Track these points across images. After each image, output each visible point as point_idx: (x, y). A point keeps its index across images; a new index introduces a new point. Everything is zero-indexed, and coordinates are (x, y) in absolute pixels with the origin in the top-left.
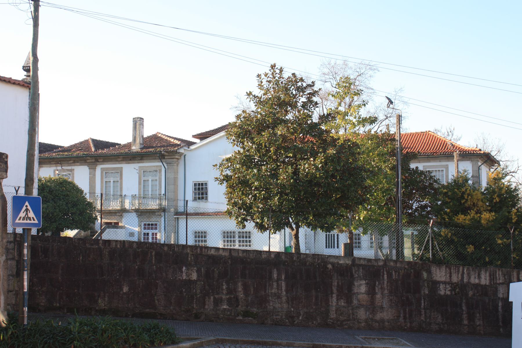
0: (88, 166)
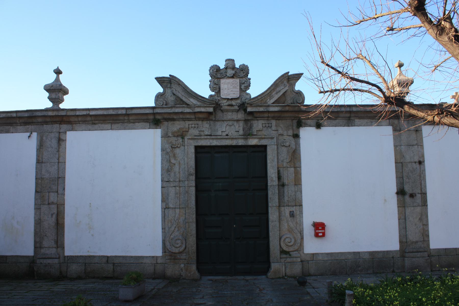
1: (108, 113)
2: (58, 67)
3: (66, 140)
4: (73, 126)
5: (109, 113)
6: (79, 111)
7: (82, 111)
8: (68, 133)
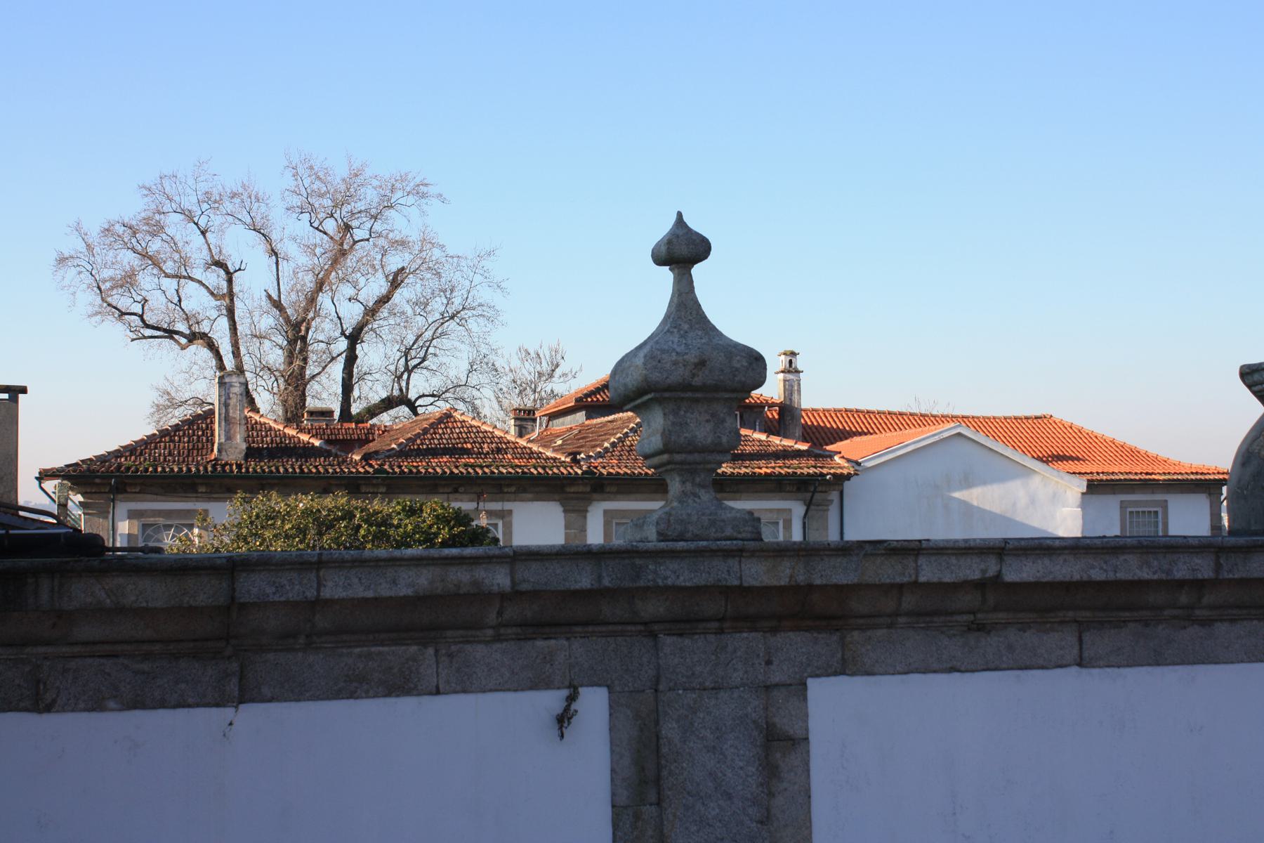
0: (562, 505)
1: (1111, 576)
2: (680, 215)
3: (806, 739)
4: (848, 639)
5: (1121, 575)
6: (933, 558)
7: (953, 560)
8: (816, 687)
